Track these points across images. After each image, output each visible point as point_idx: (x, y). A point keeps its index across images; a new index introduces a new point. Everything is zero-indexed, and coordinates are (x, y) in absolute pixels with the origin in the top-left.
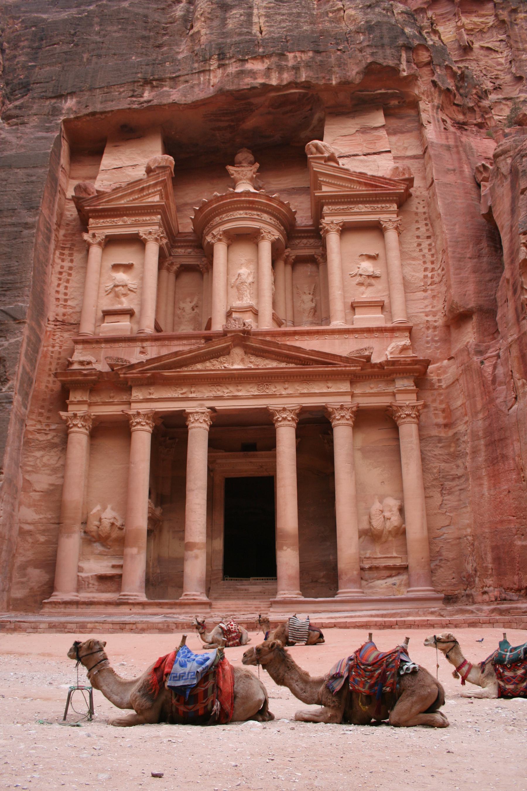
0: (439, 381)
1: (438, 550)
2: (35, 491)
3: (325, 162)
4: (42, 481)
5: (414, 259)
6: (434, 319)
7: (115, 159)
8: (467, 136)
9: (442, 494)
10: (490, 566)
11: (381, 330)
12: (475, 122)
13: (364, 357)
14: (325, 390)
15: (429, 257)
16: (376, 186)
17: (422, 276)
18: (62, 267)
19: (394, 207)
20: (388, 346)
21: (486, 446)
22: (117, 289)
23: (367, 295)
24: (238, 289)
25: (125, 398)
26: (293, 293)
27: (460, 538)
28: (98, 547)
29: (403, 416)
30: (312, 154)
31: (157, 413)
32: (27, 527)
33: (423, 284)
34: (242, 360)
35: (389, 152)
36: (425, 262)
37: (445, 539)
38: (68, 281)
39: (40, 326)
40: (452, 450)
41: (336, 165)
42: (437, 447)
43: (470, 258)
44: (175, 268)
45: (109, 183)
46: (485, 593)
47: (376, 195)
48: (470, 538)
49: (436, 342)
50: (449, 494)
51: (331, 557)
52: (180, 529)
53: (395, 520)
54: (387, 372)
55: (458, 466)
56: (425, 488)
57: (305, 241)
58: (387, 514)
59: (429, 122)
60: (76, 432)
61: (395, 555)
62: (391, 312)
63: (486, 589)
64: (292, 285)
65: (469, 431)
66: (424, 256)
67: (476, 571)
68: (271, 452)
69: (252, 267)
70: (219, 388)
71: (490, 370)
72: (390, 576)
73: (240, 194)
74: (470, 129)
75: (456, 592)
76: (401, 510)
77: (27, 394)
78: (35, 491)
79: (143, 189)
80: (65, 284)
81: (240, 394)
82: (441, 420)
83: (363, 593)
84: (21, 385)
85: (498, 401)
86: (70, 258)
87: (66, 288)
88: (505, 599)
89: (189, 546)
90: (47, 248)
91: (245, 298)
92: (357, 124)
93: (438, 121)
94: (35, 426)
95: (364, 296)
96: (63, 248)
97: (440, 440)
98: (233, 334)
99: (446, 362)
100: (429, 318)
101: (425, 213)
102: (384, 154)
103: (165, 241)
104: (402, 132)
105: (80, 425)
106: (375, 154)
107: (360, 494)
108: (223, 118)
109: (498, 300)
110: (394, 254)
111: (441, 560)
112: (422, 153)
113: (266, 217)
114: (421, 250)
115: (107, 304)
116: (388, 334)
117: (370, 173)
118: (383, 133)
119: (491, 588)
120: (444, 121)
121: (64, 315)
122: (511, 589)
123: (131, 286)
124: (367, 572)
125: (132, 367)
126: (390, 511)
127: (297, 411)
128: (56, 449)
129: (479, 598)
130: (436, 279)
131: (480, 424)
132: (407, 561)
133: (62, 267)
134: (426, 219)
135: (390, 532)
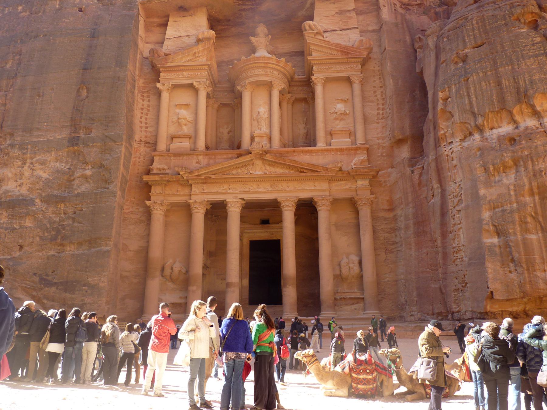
0: (385, 182)
1: (383, 288)
2: (130, 251)
3: (315, 35)
4: (134, 245)
5: (372, 102)
6: (383, 142)
7: (176, 31)
8: (410, 14)
10: (415, 299)
11: (348, 149)
12: (416, 3)
14: (313, 188)
15: (381, 101)
16: (348, 53)
17: (376, 114)
18: (143, 105)
19: (360, 66)
21: (415, 224)
22: (180, 121)
23: (340, 126)
24: (258, 122)
25: (187, 191)
26: (292, 123)
27: (397, 281)
28: (170, 285)
30: (306, 31)
31: (208, 201)
32: (125, 274)
33: (376, 118)
34: (261, 169)
35: (357, 28)
36: (378, 104)
37: (388, 281)
38: (147, 115)
39: (131, 145)
40: (392, 225)
41: (322, 38)
43: (408, 102)
44: (216, 105)
45: (173, 48)
46: (412, 315)
47: (347, 58)
48: (403, 281)
49: (384, 156)
50: (390, 253)
51: (316, 291)
52: (223, 274)
53: (356, 269)
55: (396, 236)
56: (375, 250)
57: (301, 88)
58: (351, 265)
59: (384, 6)
60: (156, 214)
61: (356, 291)
62: (355, 137)
63: (413, 313)
64: (292, 118)
65: (403, 214)
66: (378, 100)
67: (406, 301)
68: (278, 225)
69: (267, 107)
70: (247, 186)
71: (417, 177)
72: (353, 304)
73: (258, 58)
74: (412, 8)
75: (394, 314)
76: (360, 263)
77: (124, 190)
78: (130, 251)
79: (195, 53)
80: (145, 116)
81: (260, 190)
82: (386, 207)
83: (336, 314)
84: (121, 185)
85: (421, 197)
86: (147, 99)
87: (146, 119)
88: (424, 320)
89: (228, 285)
90: (133, 93)
91: (262, 128)
93: (391, 5)
94: (129, 209)
95: (339, 127)
96: (143, 92)
97: (385, 219)
98: (255, 152)
99: (390, 170)
100: (380, 141)
101: (379, 70)
102: (353, 30)
103: (210, 89)
104: (366, 13)
105: (159, 209)
106: (347, 29)
107: (334, 252)
108: (247, 3)
109: (425, 131)
110: (358, 100)
111: (385, 294)
112: (379, 28)
113: (275, 72)
114: (376, 96)
115: (173, 130)
116: (353, 152)
117: (344, 44)
118: (353, 14)
119: (416, 313)
120: (395, 4)
121: (146, 137)
122: (428, 314)
123: (189, 119)
124: (338, 301)
125: (191, 172)
126: (353, 263)
127: (296, 201)
128: (143, 224)
129: (409, 319)
130: (385, 116)
131: (410, 211)
132: (363, 294)
133: (143, 105)
134: (380, 75)
135: (353, 276)
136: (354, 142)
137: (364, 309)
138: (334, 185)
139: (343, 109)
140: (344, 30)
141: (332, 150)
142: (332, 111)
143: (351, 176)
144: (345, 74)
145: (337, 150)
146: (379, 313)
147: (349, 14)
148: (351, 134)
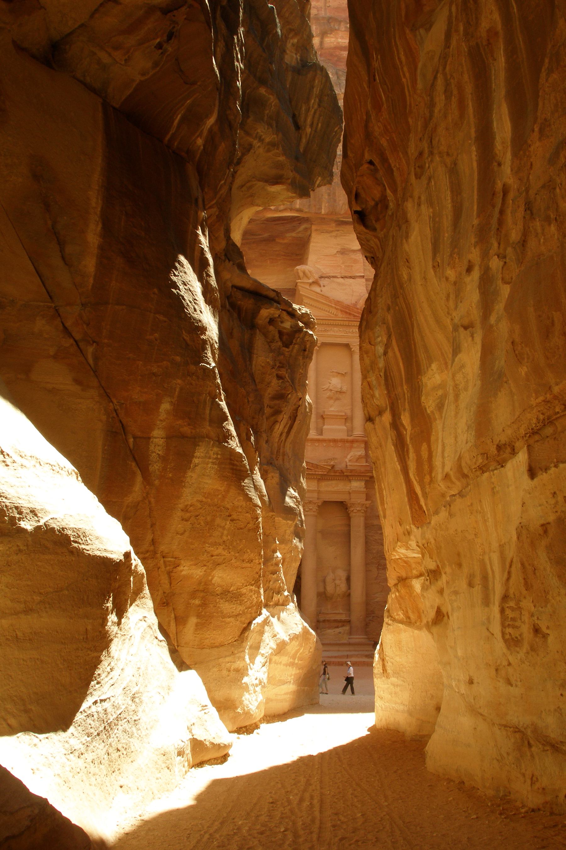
9: (378, 569)
13: (329, 465)
20: (348, 455)
29: (355, 511)
35: (363, 277)
42: (377, 533)
53: (343, 587)
54: (345, 475)
58: (337, 582)
61: (341, 611)
72: (337, 627)
76: (348, 579)
92: (338, 244)
106: (351, 277)
111: (373, 617)
126: (340, 580)
135: (339, 595)
136: (350, 431)
137: (350, 633)
138: (323, 484)
139: (339, 386)
140: (346, 277)
141: (324, 441)
142: (326, 387)
143: (345, 475)
144: (344, 341)
145: (330, 441)
146: (365, 638)
147: (353, 256)
148: (348, 419)
